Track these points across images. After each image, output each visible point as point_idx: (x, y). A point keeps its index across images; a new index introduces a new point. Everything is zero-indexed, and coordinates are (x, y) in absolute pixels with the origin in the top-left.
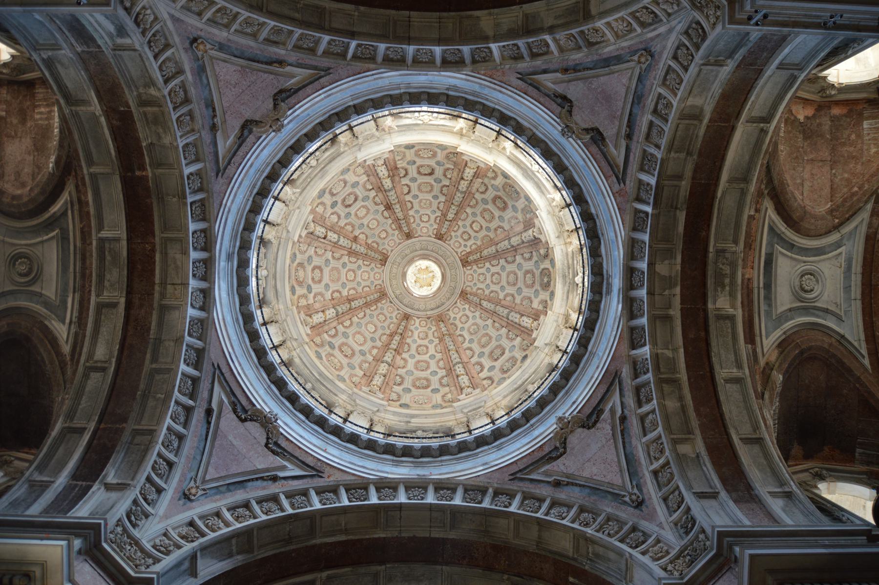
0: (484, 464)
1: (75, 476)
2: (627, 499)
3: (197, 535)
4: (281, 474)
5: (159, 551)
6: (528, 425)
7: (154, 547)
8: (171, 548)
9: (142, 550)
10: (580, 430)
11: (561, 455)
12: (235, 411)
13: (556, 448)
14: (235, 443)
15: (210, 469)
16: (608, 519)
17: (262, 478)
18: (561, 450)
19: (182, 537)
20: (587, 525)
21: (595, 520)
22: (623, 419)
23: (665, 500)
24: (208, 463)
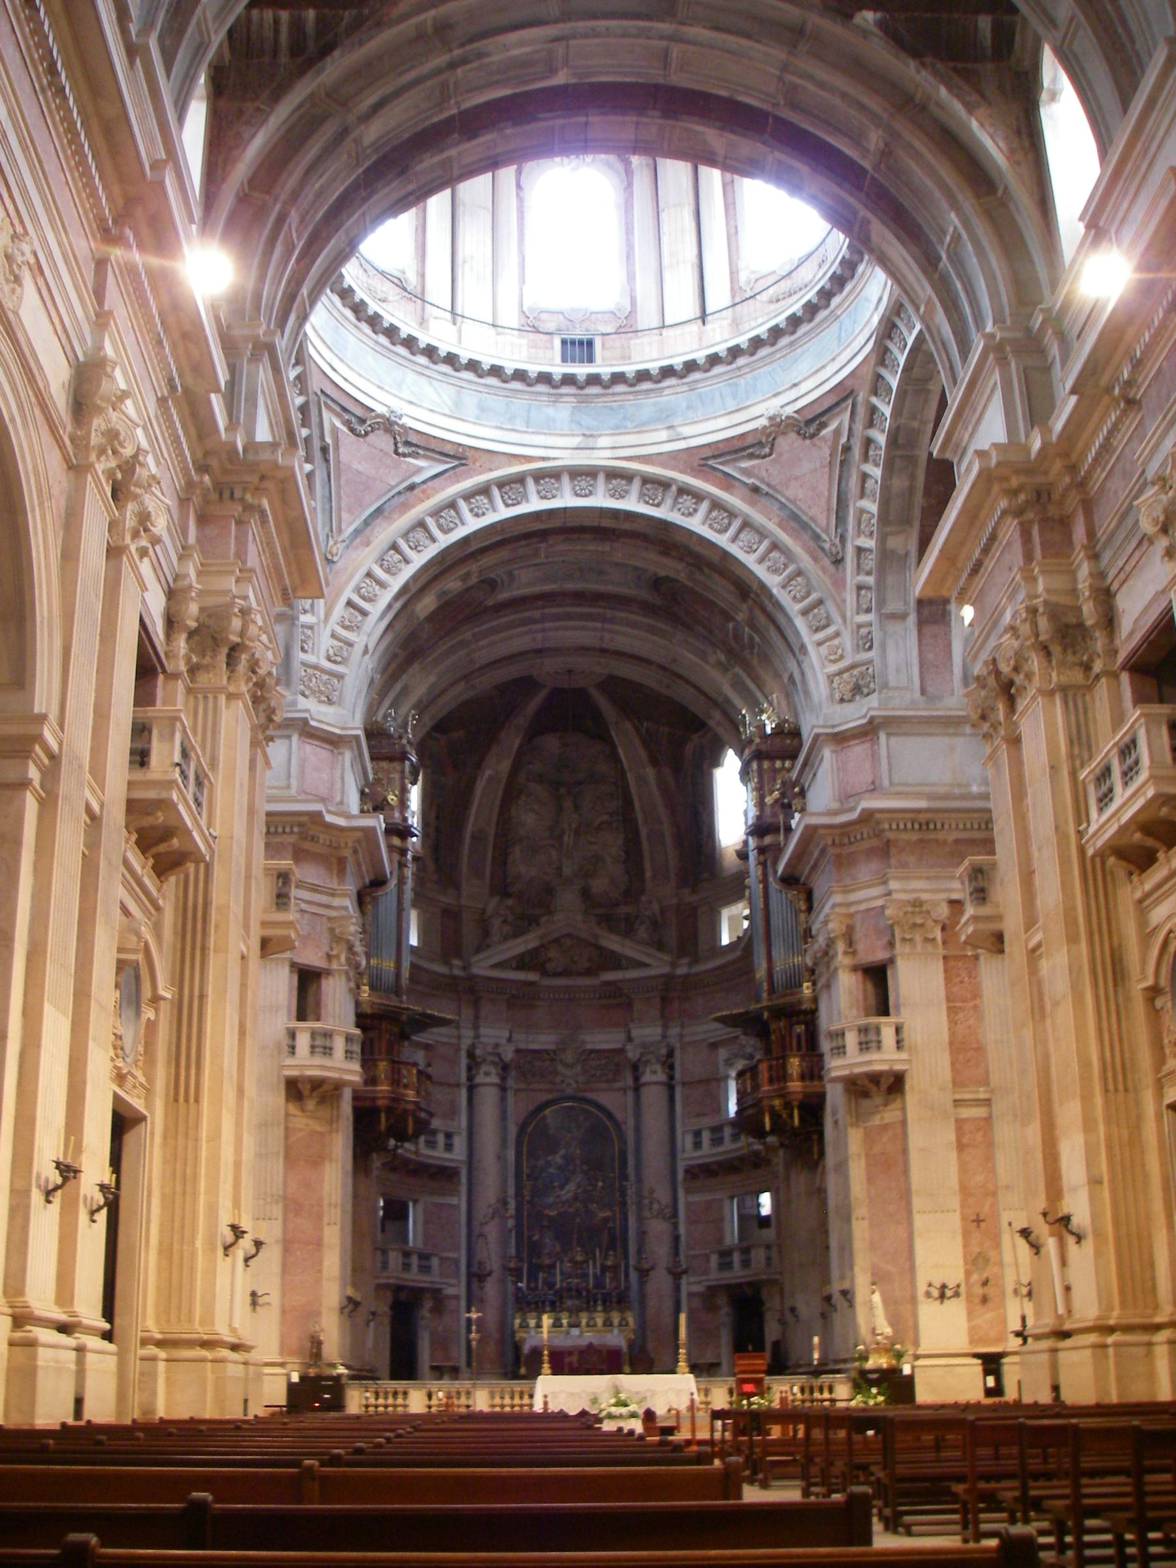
0: (671, 427)
2: (827, 546)
4: (418, 479)
5: (335, 662)
6: (734, 366)
7: (329, 659)
8: (345, 654)
9: (323, 671)
10: (793, 436)
11: (765, 457)
12: (352, 430)
13: (760, 444)
14: (361, 469)
15: (344, 516)
16: (799, 573)
17: (399, 493)
18: (767, 450)
20: (774, 571)
21: (786, 566)
22: (847, 449)
23: (859, 588)
24: (339, 509)
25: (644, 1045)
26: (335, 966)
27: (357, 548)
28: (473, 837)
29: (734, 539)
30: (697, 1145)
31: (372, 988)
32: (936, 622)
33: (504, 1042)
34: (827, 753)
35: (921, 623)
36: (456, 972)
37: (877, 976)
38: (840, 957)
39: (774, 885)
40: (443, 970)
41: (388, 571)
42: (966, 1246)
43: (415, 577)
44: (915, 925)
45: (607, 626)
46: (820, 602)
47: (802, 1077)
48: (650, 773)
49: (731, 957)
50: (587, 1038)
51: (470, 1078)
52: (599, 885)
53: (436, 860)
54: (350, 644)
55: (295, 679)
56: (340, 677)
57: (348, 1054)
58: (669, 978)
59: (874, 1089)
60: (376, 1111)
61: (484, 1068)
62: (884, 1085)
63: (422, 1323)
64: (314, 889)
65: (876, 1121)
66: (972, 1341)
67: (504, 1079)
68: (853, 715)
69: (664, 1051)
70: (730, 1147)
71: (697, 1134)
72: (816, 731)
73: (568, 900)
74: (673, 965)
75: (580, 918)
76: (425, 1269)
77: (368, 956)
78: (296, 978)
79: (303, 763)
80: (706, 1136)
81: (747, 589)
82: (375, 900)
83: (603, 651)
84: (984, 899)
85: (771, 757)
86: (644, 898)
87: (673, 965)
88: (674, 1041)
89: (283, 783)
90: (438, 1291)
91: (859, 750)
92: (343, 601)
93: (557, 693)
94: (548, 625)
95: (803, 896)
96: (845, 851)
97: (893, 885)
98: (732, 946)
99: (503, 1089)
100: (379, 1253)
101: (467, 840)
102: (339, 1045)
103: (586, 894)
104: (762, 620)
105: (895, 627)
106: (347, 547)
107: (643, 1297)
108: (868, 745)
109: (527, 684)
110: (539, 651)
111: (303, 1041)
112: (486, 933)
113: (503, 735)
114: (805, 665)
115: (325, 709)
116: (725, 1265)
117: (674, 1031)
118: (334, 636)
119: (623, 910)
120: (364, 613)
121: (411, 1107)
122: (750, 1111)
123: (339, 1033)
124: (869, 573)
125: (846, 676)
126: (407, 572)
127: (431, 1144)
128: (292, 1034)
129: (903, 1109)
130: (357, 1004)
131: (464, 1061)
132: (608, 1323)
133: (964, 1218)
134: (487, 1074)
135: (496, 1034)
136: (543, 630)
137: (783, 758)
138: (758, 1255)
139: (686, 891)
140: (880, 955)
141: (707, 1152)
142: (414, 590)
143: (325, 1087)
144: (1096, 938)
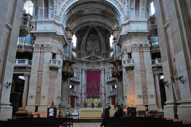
1: (45, 7)
2: (123, 1)
3: (63, 10)
7: (59, 15)
9: (58, 17)
16: (120, 5)
19: (61, 12)
20: (116, 5)
23: (127, 6)
25: (101, 68)
26: (58, 53)
27: (63, 2)
28: (82, 45)
29: (111, 1)
30: (108, 79)
31: (65, 58)
32: (138, 10)
33: (85, 68)
34: (123, 27)
35: (136, 10)
36: (80, 60)
37: (130, 55)
38: (125, 52)
39: (116, 46)
40: (78, 59)
41: (67, 5)
42: (143, 90)
43: (71, 6)
44: (135, 47)
45: (97, 18)
46: (122, 9)
47: (120, 69)
48: (102, 38)
49: (111, 58)
50: (95, 68)
51: (82, 72)
52: (97, 51)
53: (78, 48)
54: (62, 14)
55: (54, 17)
56: (61, 18)
57: (58, 64)
58: (104, 60)
59: (130, 69)
60: (65, 73)
61: (83, 71)
62: (131, 69)
63: (75, 100)
64: (55, 43)
65: (130, 73)
66: (144, 103)
67: (86, 72)
68: (127, 22)
69: (104, 69)
70: (111, 79)
71: (108, 78)
72: (122, 24)
73: (93, 52)
74: (105, 59)
75: (94, 54)
76: (75, 94)
77: (65, 54)
78: (52, 54)
79: (54, 28)
80: (109, 78)
81: (113, 9)
82: (66, 47)
83: (97, 22)
84: (153, 23)
85: (116, 31)
86: (102, 52)
87: (105, 59)
88: (105, 68)
89: (52, 29)
90: (77, 96)
91: (127, 26)
92: (61, 8)
93: (92, 28)
94: (90, 18)
95: (120, 46)
96: (126, 39)
97: (132, 42)
98: (112, 57)
99: (85, 73)
100: (69, 92)
101: (82, 45)
102: (57, 62)
103: (95, 51)
104: (115, 13)
105: (132, 10)
106: (62, 2)
107: (101, 97)
108: (128, 25)
109: (87, 27)
110: (89, 22)
111: (52, 62)
112: (84, 55)
113: (86, 33)
114: (120, 17)
115: (59, 21)
116: (110, 94)
117: (105, 67)
118: (60, 12)
119: (100, 53)
120: (64, 10)
121: (69, 72)
122: (113, 74)
123: (57, 61)
124: (129, 4)
125: (126, 17)
126: (70, 5)
127: (77, 79)
128: (51, 61)
129: (134, 71)
130: (63, 59)
131: (81, 70)
132: (97, 100)
133: (142, 86)
134: (84, 71)
135: (85, 67)
136: (89, 19)
137: (117, 31)
138: (115, 92)
139: (107, 51)
140: (130, 51)
141: (109, 80)
142: (71, 8)
143: (55, 68)
144: (185, 16)
